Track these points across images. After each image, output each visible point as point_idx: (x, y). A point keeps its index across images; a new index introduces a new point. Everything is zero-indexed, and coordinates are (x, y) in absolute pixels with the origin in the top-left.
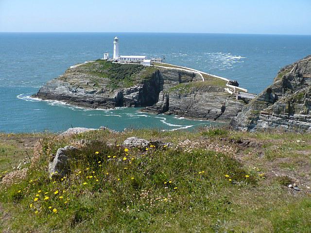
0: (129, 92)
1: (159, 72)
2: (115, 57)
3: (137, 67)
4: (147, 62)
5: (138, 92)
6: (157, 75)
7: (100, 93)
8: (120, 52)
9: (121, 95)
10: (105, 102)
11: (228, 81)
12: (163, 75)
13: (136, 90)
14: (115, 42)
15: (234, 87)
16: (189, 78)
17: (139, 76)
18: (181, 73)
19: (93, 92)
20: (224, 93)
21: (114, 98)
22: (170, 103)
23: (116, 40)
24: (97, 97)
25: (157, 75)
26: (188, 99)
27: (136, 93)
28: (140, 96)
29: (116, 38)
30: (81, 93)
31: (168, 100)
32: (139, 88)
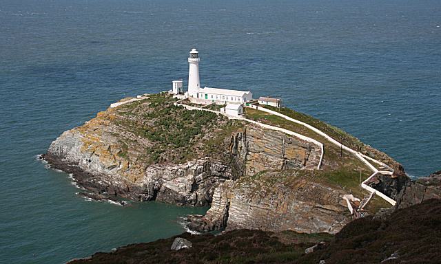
4: (232, 112)
5: (191, 177)
6: (241, 143)
7: (122, 171)
8: (205, 81)
10: (128, 191)
11: (376, 171)
14: (190, 60)
15: (373, 190)
16: (302, 153)
20: (336, 209)
21: (142, 184)
22: (230, 214)
23: (195, 56)
28: (195, 187)
29: (194, 51)
30: (97, 166)
31: (228, 207)
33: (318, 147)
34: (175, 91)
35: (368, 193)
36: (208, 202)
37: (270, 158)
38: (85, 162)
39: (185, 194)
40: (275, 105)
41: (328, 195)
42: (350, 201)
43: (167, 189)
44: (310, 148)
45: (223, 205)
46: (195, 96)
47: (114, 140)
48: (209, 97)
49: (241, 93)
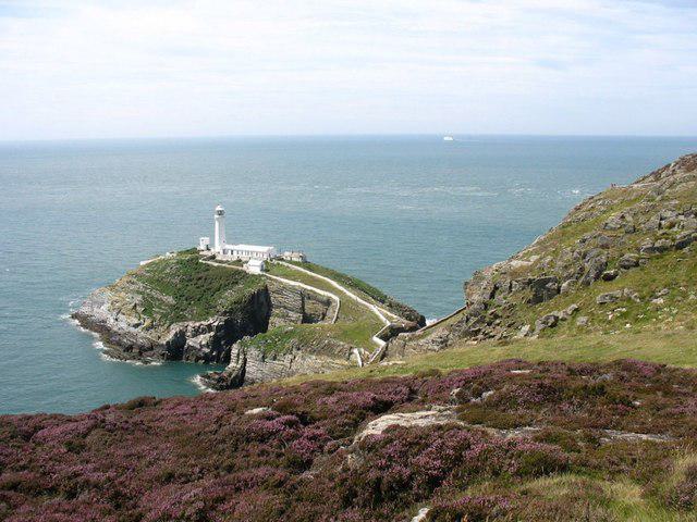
0: (197, 332)
1: (266, 289)
2: (217, 249)
3: (235, 275)
4: (254, 268)
5: (212, 334)
6: (262, 299)
7: (148, 329)
9: (181, 337)
10: (151, 348)
11: (388, 324)
12: (275, 298)
13: (210, 327)
16: (321, 308)
17: (229, 297)
18: (304, 296)
19: (136, 326)
24: (142, 337)
25: (262, 299)
26: (277, 365)
27: (208, 335)
29: (219, 208)
32: (216, 324)
33: (335, 301)
34: (202, 247)
35: (378, 346)
36: (227, 360)
37: (291, 313)
38: (112, 321)
39: (207, 350)
40: (295, 259)
41: (339, 349)
42: (360, 353)
43: (189, 346)
44: (328, 303)
45: (240, 362)
46: (221, 252)
47: (140, 297)
48: (235, 253)
49: (265, 249)
